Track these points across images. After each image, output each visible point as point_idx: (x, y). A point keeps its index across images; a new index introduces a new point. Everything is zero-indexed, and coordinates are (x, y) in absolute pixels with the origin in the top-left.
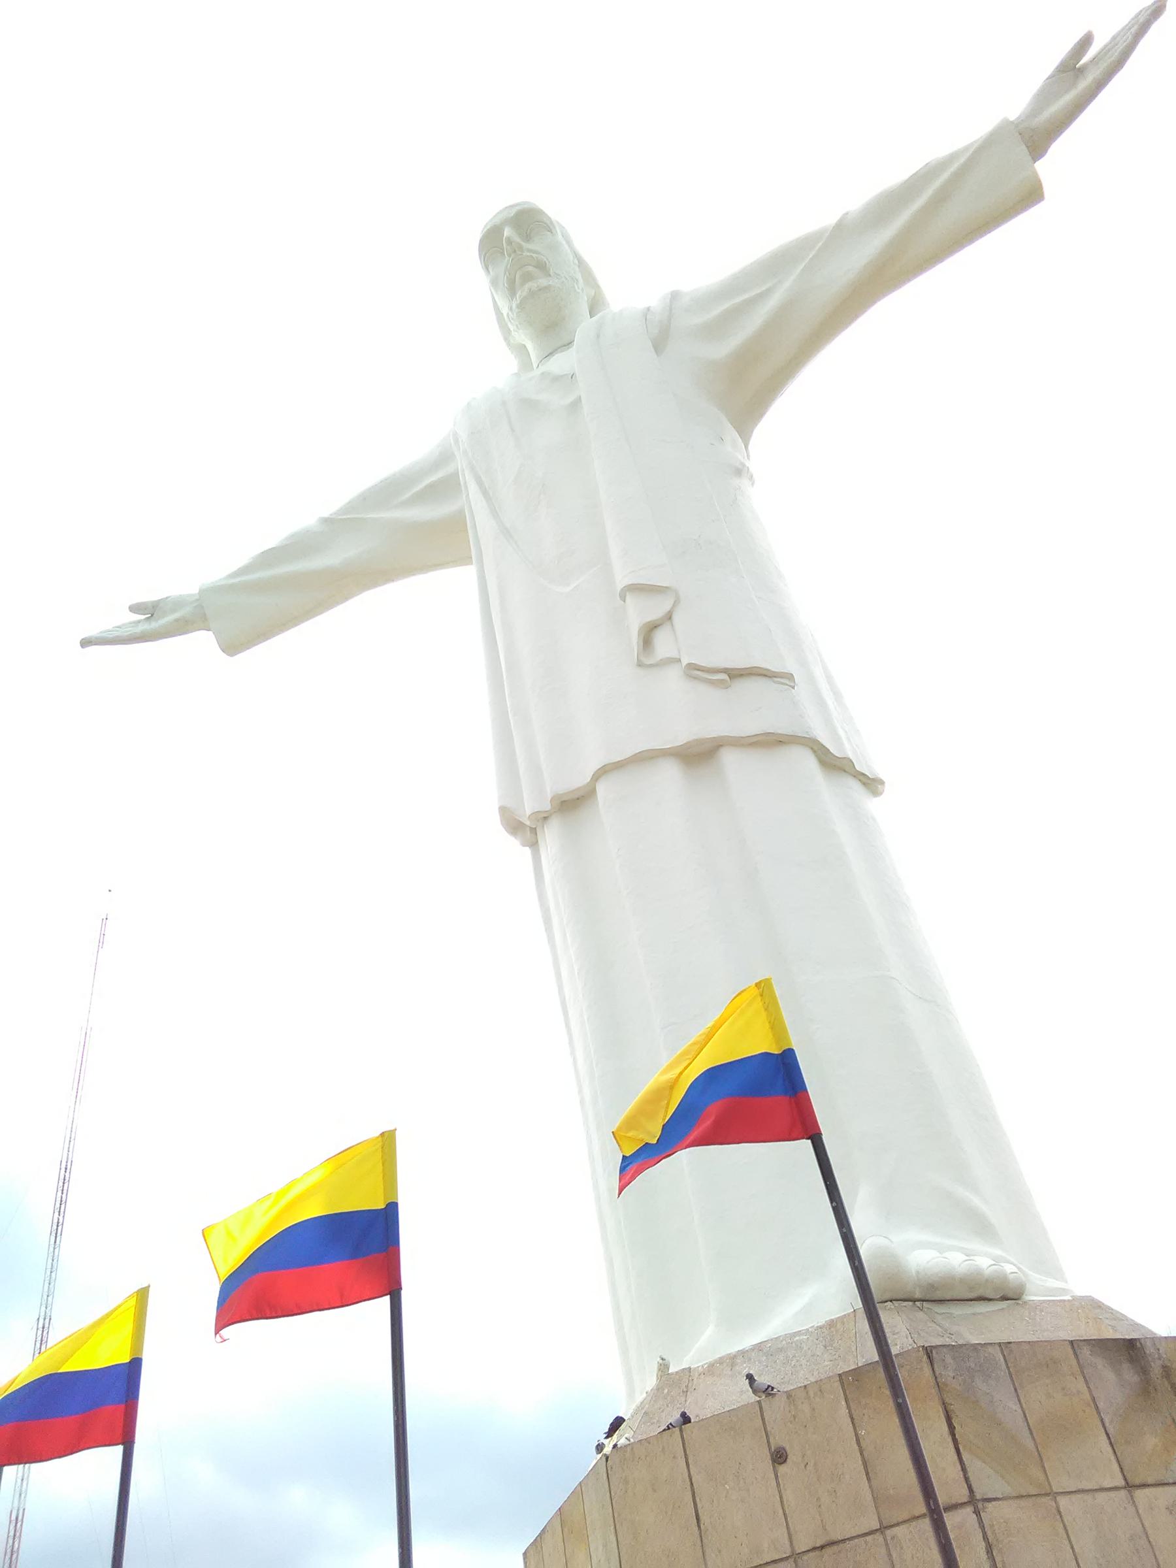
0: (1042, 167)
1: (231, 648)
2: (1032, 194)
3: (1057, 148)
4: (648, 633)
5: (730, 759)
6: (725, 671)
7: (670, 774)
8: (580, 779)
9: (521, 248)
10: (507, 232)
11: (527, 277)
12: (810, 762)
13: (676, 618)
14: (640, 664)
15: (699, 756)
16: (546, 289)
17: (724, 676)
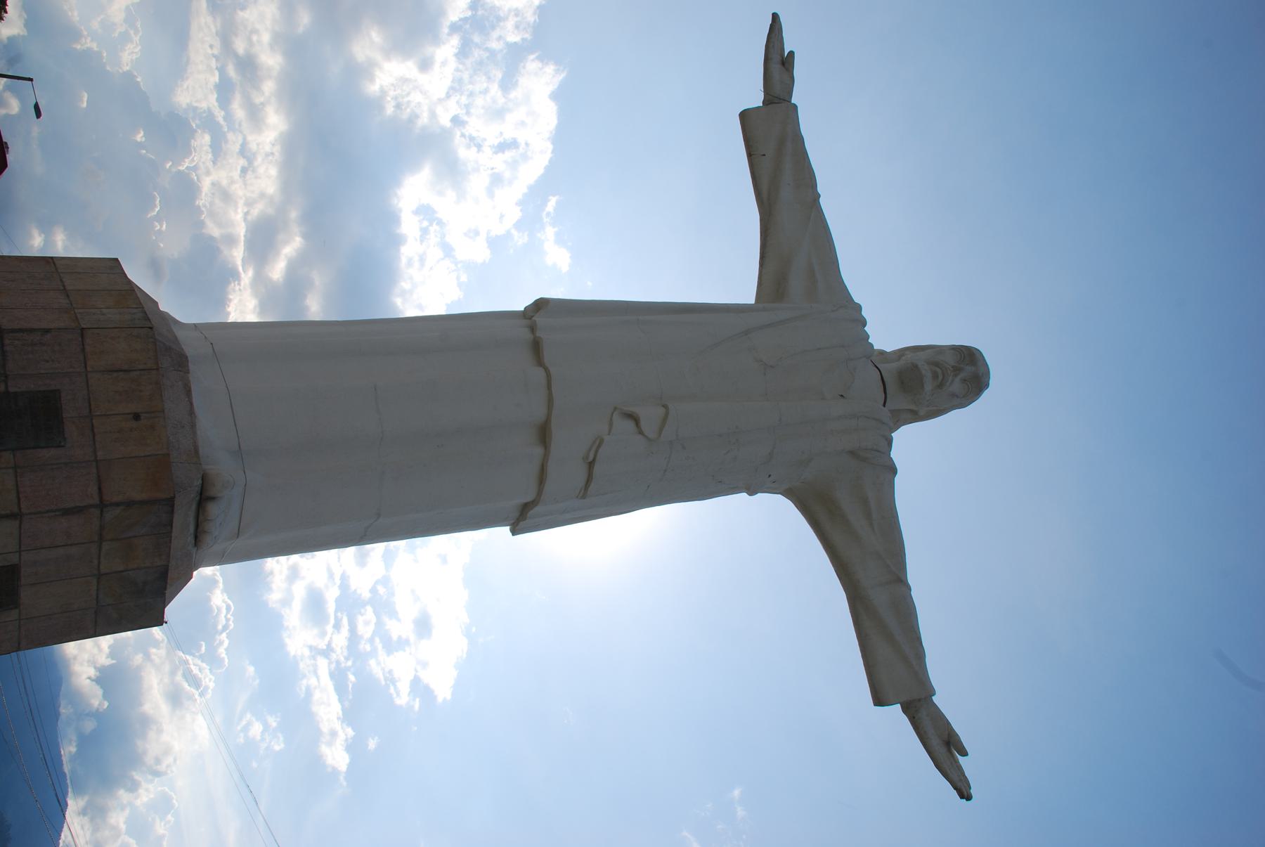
0: (897, 708)
1: (745, 116)
2: (879, 700)
3: (904, 719)
5: (539, 451)
8: (547, 360)
9: (956, 375)
10: (969, 369)
11: (935, 376)
12: (529, 498)
14: (615, 409)
15: (544, 434)
17: (591, 459)
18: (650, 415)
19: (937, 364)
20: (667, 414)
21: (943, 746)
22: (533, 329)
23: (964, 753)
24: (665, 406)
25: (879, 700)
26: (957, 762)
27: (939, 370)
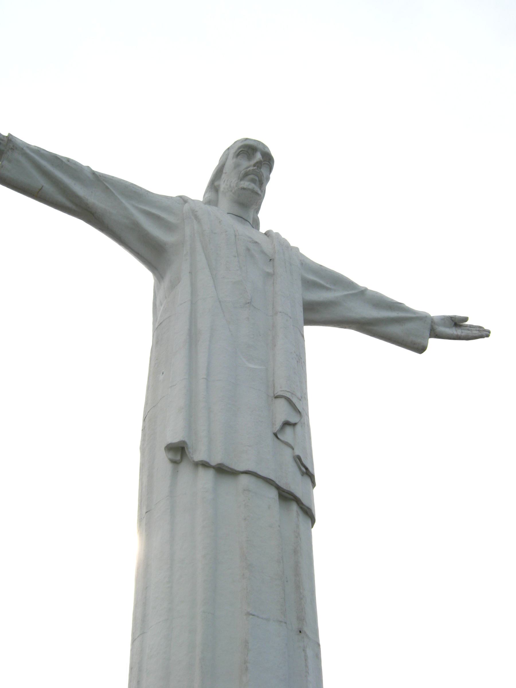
2: (420, 349)
4: (287, 424)
6: (307, 469)
7: (273, 494)
10: (258, 156)
11: (253, 181)
13: (298, 428)
14: (276, 435)
15: (286, 497)
16: (257, 193)
18: (283, 411)
19: (246, 175)
20: (289, 400)
21: (457, 328)
22: (205, 465)
23: (466, 319)
24: (276, 397)
25: (420, 349)
26: (466, 326)
27: (252, 176)
